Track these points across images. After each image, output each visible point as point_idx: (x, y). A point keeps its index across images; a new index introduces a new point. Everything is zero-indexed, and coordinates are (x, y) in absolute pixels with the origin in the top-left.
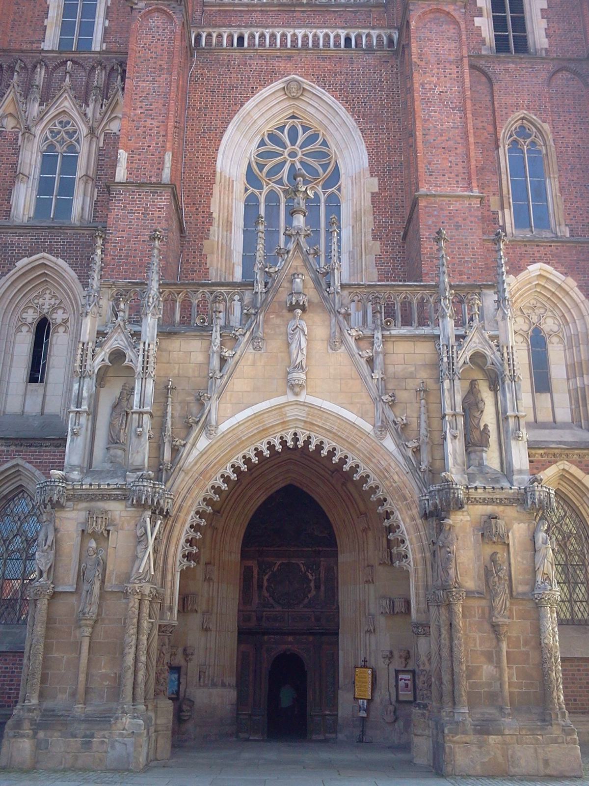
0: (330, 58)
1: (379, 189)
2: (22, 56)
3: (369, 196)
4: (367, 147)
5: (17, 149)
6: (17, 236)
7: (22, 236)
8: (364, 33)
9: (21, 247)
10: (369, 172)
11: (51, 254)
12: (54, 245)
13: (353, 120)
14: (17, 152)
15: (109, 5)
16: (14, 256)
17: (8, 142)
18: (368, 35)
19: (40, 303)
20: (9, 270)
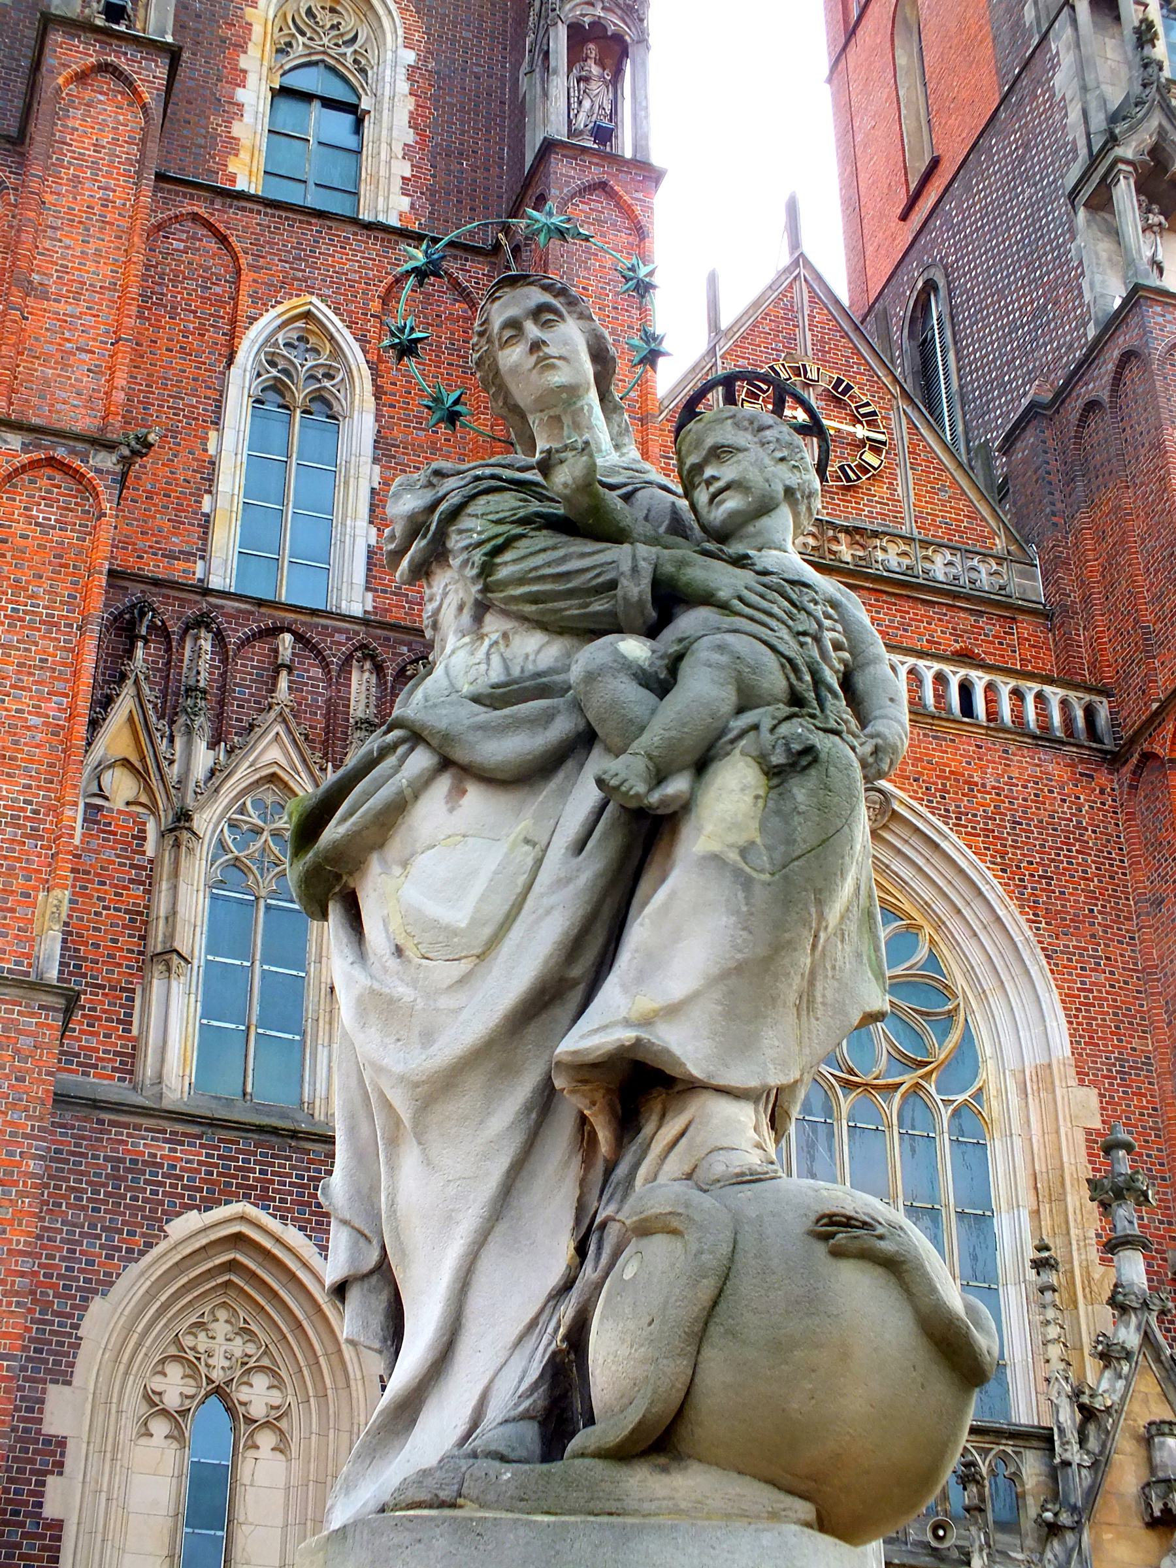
0: (953, 741)
1: (1103, 1122)
2: (154, 595)
3: (1081, 1137)
4: (1063, 1001)
5: (145, 868)
6: (166, 1141)
7: (182, 1143)
8: (1030, 689)
9: (181, 1178)
10: (1072, 1072)
11: (265, 1208)
12: (272, 1182)
13: (1021, 920)
14: (147, 876)
15: (376, 486)
16: (162, 1203)
17: (115, 841)
18: (1040, 697)
19: (201, 1349)
20: (149, 1245)
